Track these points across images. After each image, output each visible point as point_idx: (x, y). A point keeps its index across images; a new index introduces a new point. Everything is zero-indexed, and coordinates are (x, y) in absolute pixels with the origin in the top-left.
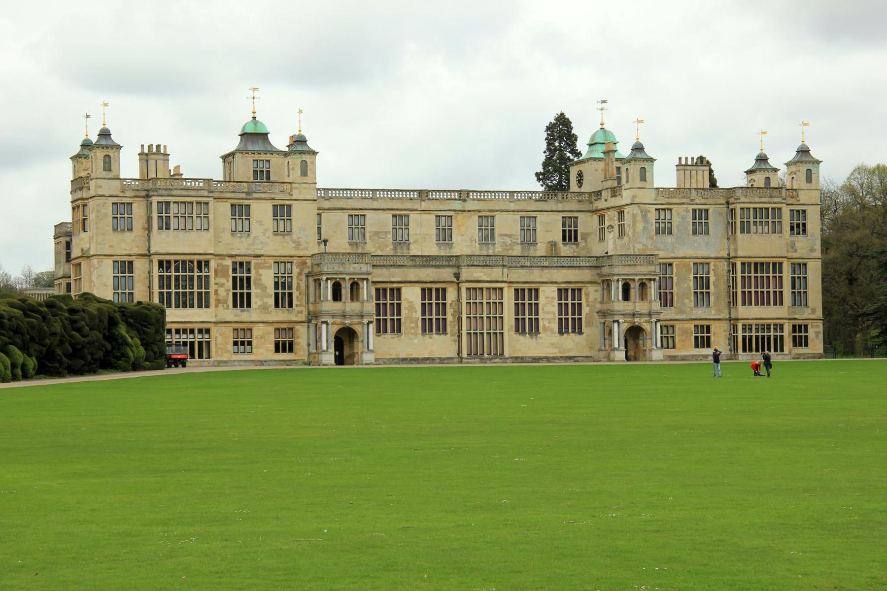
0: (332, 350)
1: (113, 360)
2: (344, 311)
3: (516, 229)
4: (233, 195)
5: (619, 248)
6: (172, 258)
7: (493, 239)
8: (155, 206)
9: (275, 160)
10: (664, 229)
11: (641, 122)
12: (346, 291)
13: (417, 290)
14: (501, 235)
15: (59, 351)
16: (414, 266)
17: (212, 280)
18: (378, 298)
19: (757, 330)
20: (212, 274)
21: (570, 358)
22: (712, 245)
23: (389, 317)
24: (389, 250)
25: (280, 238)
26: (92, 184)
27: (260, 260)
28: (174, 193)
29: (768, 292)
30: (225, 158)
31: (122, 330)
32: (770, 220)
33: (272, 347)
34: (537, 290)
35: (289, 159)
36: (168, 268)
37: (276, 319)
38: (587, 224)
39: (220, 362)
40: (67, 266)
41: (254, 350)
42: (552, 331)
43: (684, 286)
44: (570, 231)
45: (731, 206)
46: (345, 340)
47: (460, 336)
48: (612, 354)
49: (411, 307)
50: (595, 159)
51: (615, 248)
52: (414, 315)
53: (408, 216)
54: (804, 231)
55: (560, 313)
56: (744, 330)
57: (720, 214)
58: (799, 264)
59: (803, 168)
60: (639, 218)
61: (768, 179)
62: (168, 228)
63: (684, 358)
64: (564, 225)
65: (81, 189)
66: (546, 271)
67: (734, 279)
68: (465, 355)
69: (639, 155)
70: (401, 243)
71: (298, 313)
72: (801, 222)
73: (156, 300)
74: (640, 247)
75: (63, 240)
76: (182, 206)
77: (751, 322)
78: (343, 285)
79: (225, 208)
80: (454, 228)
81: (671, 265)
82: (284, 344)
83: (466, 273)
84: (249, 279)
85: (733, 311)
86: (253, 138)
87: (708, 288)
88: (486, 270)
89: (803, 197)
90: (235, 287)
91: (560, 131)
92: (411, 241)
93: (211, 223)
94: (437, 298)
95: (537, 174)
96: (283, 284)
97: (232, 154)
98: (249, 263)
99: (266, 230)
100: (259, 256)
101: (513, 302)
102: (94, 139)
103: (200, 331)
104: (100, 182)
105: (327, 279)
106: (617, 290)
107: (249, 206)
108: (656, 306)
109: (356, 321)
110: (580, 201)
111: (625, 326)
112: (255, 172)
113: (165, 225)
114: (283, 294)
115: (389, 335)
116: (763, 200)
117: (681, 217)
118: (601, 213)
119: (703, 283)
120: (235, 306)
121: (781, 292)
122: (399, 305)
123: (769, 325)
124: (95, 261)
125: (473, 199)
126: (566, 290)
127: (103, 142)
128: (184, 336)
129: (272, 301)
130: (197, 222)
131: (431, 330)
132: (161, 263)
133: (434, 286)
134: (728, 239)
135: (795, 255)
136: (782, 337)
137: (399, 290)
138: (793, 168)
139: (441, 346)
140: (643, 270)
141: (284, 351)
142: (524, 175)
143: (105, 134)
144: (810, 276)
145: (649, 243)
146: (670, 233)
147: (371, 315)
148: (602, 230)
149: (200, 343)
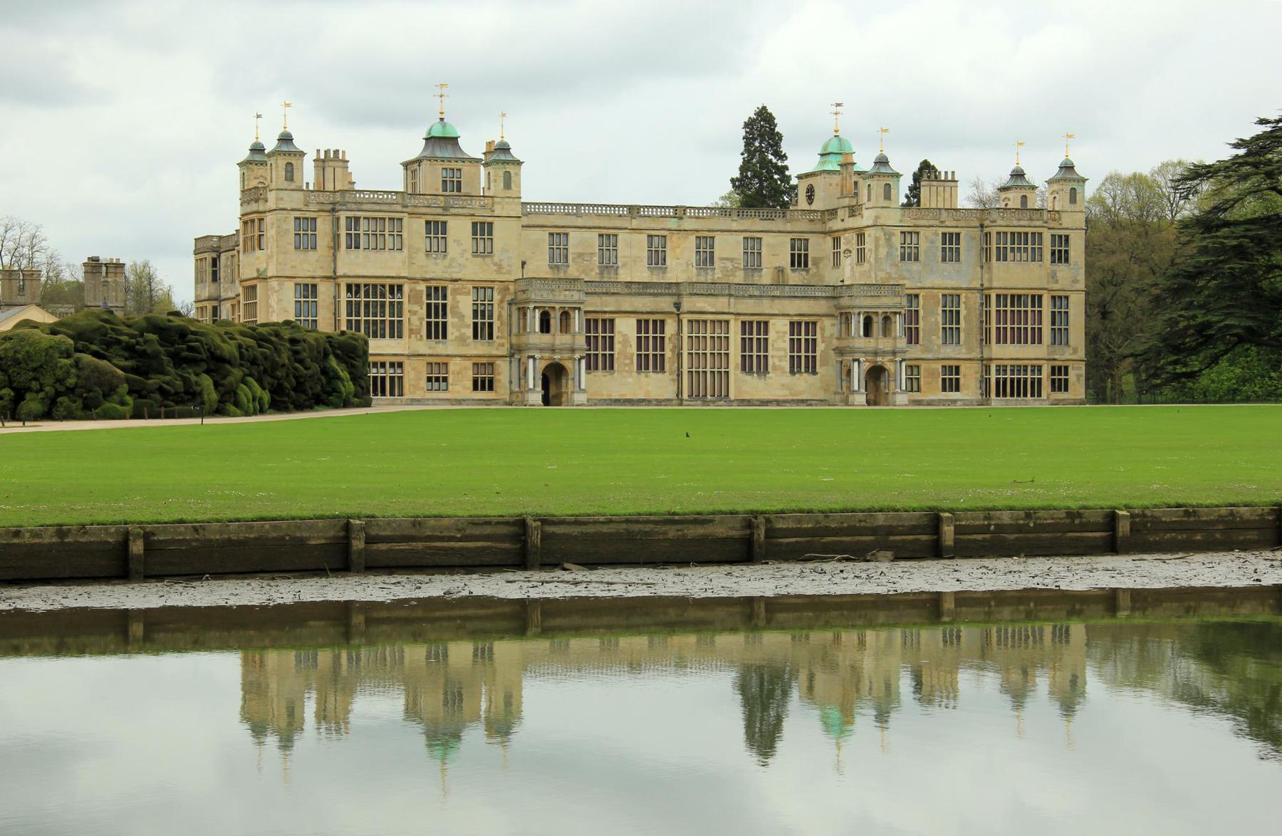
0: (539, 388)
1: (324, 396)
2: (553, 345)
3: (738, 252)
4: (427, 210)
5: (857, 275)
6: (362, 281)
7: (712, 263)
8: (343, 222)
9: (466, 168)
10: (910, 255)
11: (886, 131)
12: (555, 322)
13: (632, 322)
14: (722, 259)
15: (286, 385)
16: (629, 294)
17: (406, 306)
18: (588, 331)
19: (1012, 372)
20: (405, 300)
21: (803, 401)
22: (962, 275)
23: (600, 352)
24: (594, 275)
25: (480, 259)
26: (272, 196)
27: (457, 285)
28: (365, 207)
29: (1026, 329)
30: (406, 165)
31: (333, 362)
32: (1030, 246)
33: (470, 384)
34: (766, 323)
35: (491, 169)
36: (358, 292)
37: (474, 352)
38: (819, 247)
39: (412, 400)
40: (213, 286)
41: (450, 388)
42: (782, 369)
43: (931, 320)
44: (800, 255)
45: (986, 230)
46: (553, 376)
47: (680, 375)
48: (851, 397)
49: (626, 341)
50: (829, 172)
51: (853, 276)
52: (629, 350)
53: (616, 236)
54: (1067, 260)
55: (792, 350)
56: (998, 371)
57: (973, 238)
58: (1060, 297)
59: (1067, 187)
60: (882, 242)
61: (1024, 197)
62: (357, 247)
63: (930, 403)
64: (793, 248)
65: (257, 201)
66: (777, 301)
67: (988, 314)
68: (685, 396)
69: (883, 170)
71: (498, 346)
72: (1063, 248)
73: (344, 328)
74: (882, 275)
75: (209, 256)
76: (372, 223)
77: (1006, 363)
78: (552, 315)
79: (420, 224)
80: (668, 249)
81: (917, 296)
82: (483, 381)
83: (687, 304)
84: (444, 306)
85: (986, 350)
86: (442, 142)
87: (958, 323)
88: (710, 299)
89: (1066, 221)
90: (429, 316)
91: (762, 132)
92: (620, 264)
93: (406, 242)
94: (655, 332)
95: (733, 180)
96: (483, 312)
97: (418, 161)
98: (444, 289)
99: (465, 251)
100: (456, 280)
101: (740, 336)
102: (270, 145)
103: (392, 365)
104: (282, 194)
105: (535, 308)
106: (857, 325)
107: (444, 223)
108: (902, 343)
109: (566, 356)
110: (811, 221)
111: (866, 366)
112: (445, 182)
113: (354, 243)
114: (483, 324)
115: (600, 373)
116: (1022, 223)
117: (930, 241)
118: (836, 235)
119: (952, 316)
120: (429, 336)
121: (1040, 329)
122: (612, 338)
123: (1026, 367)
124: (274, 283)
125: (690, 217)
126: (799, 324)
127: (285, 148)
128: (374, 370)
129: (470, 332)
130: (389, 240)
131: (647, 368)
132: (349, 287)
133: (651, 317)
134: (982, 267)
135: (1056, 287)
136: (1040, 380)
137: (612, 321)
138: (1055, 187)
139: (658, 385)
140: (887, 302)
141: (483, 388)
142: (711, 178)
143: (286, 139)
144: (1072, 312)
145: (893, 271)
146: (917, 259)
147: (581, 349)
148: (836, 256)
149: (392, 379)
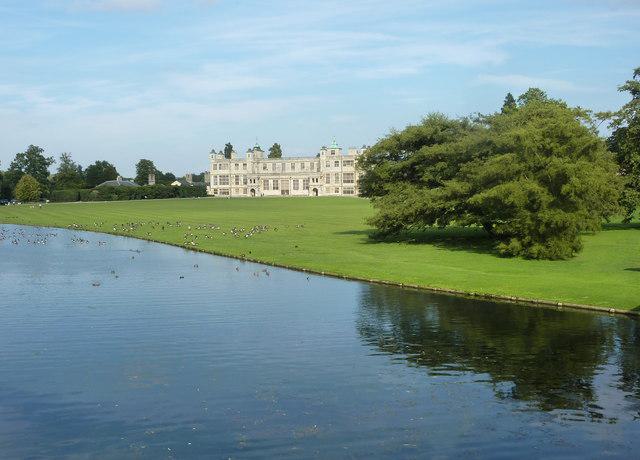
70: (283, 169)
